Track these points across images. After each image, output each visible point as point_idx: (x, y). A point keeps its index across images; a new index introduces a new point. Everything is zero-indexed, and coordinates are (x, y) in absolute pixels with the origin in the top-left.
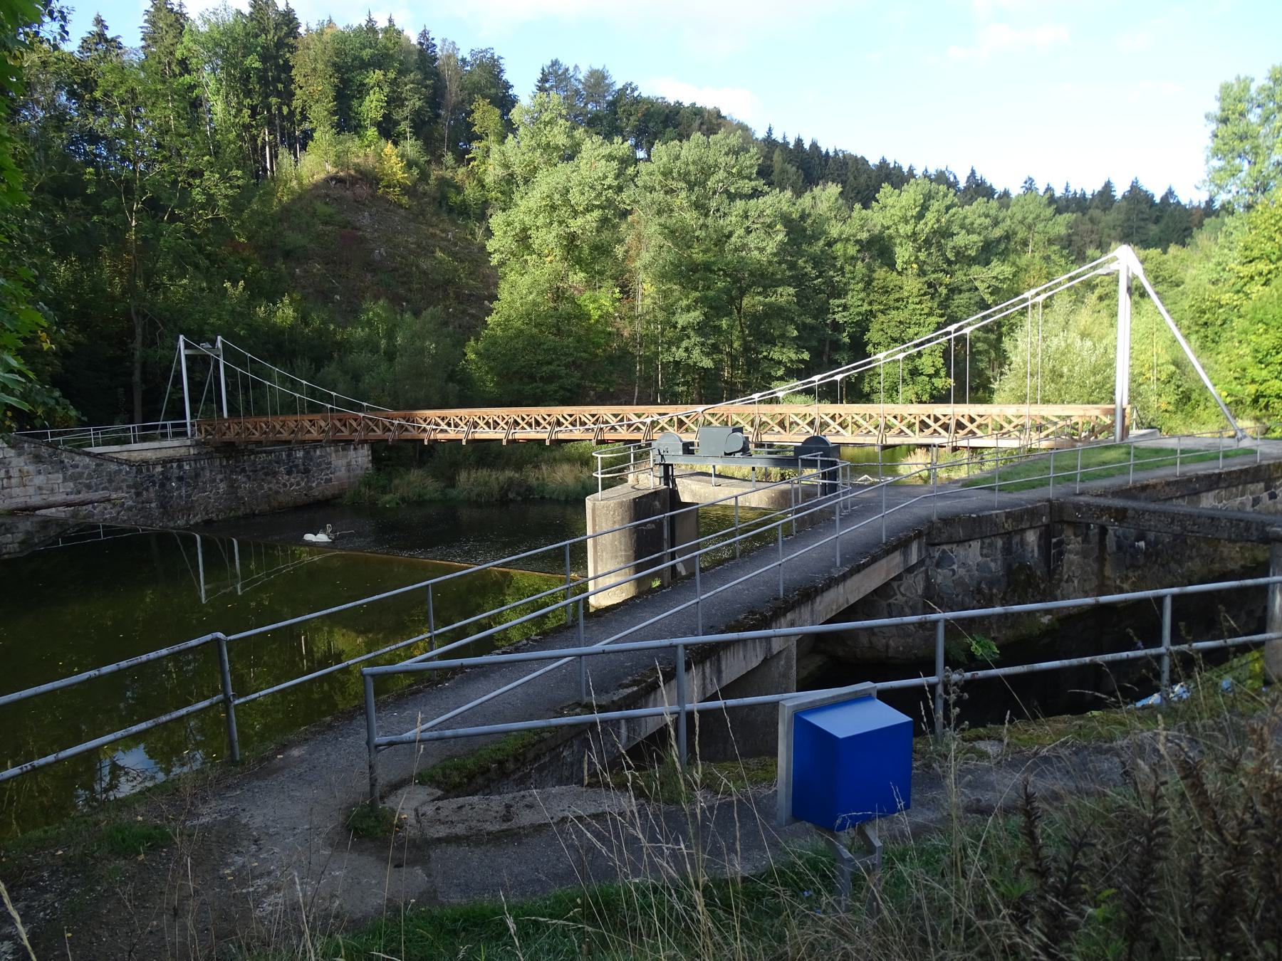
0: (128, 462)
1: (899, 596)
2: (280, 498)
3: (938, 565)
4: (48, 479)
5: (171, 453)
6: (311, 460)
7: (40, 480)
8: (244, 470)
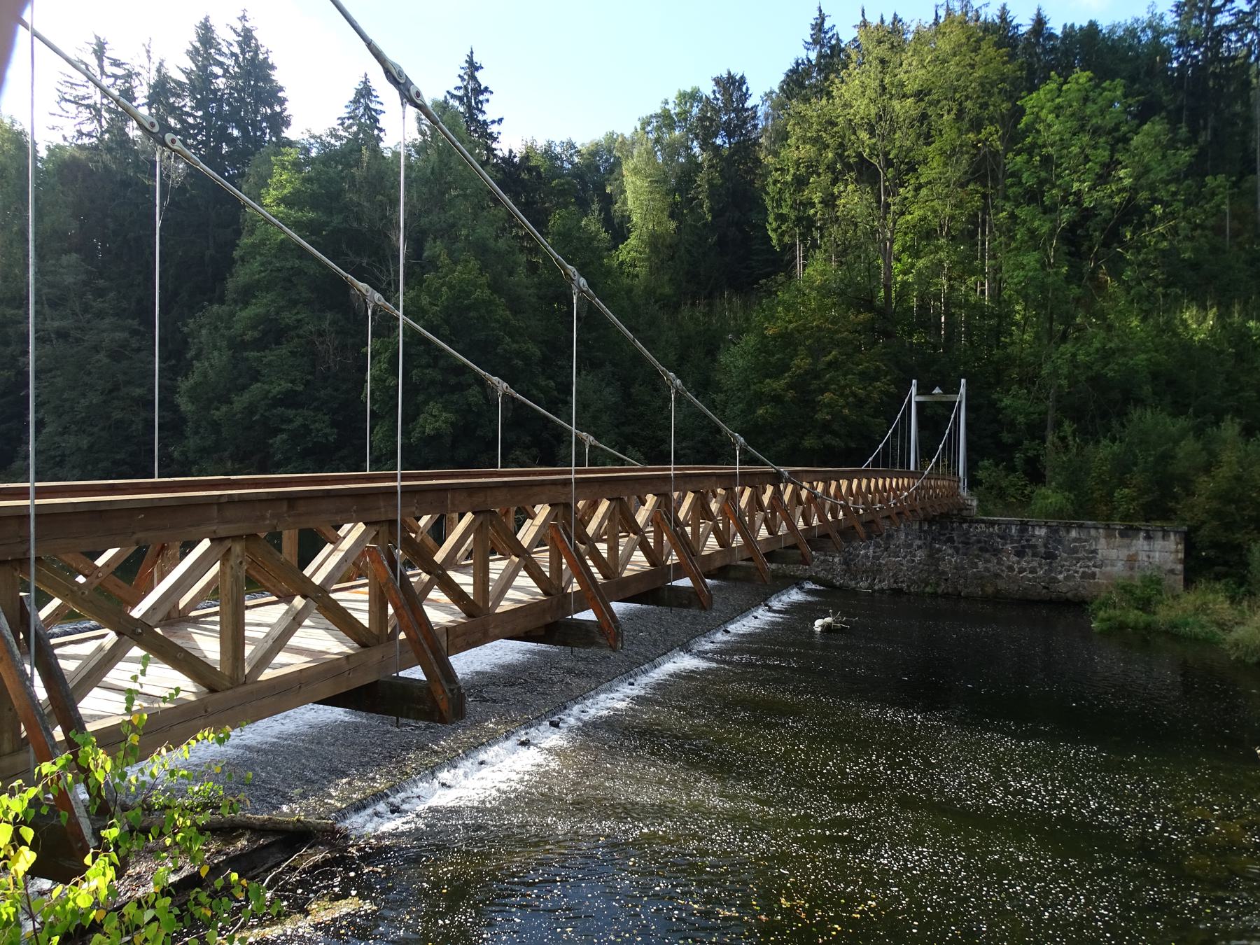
2: (1002, 585)
6: (1060, 542)
8: (950, 540)
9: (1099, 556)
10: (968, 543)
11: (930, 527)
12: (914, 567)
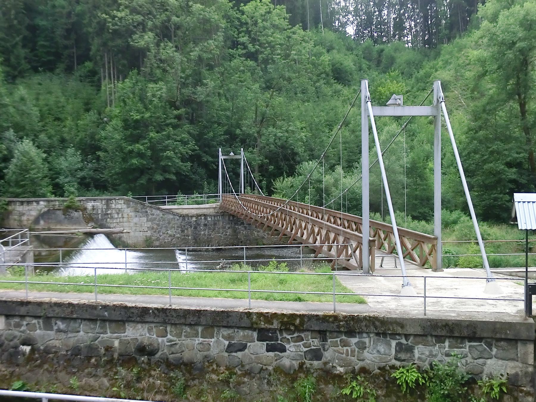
0: (177, 214)
4: (140, 220)
7: (136, 220)
12: (227, 238)
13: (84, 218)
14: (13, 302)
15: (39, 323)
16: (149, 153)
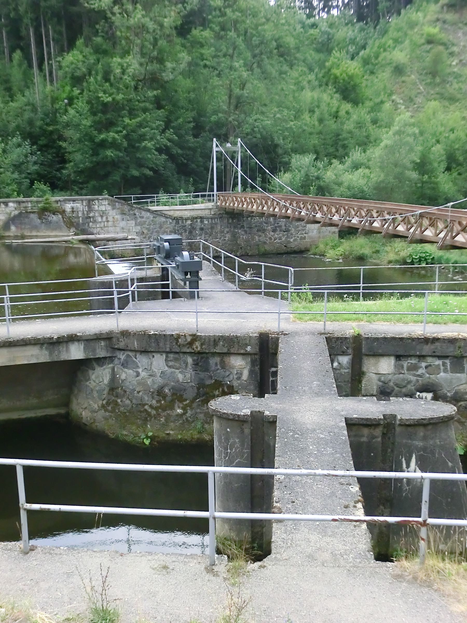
0: (170, 217)
1: (92, 382)
2: (267, 248)
3: (125, 365)
4: (127, 224)
5: (199, 213)
7: (123, 224)
8: (243, 227)
9: (307, 228)
10: (251, 228)
11: (233, 221)
13: (64, 222)
14: (413, 339)
15: (444, 364)
16: (125, 144)
